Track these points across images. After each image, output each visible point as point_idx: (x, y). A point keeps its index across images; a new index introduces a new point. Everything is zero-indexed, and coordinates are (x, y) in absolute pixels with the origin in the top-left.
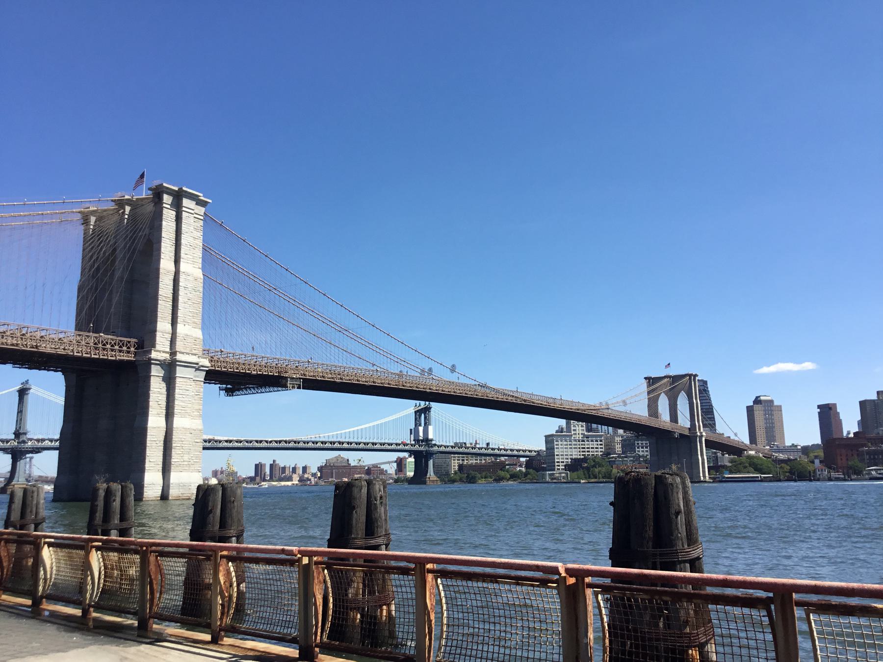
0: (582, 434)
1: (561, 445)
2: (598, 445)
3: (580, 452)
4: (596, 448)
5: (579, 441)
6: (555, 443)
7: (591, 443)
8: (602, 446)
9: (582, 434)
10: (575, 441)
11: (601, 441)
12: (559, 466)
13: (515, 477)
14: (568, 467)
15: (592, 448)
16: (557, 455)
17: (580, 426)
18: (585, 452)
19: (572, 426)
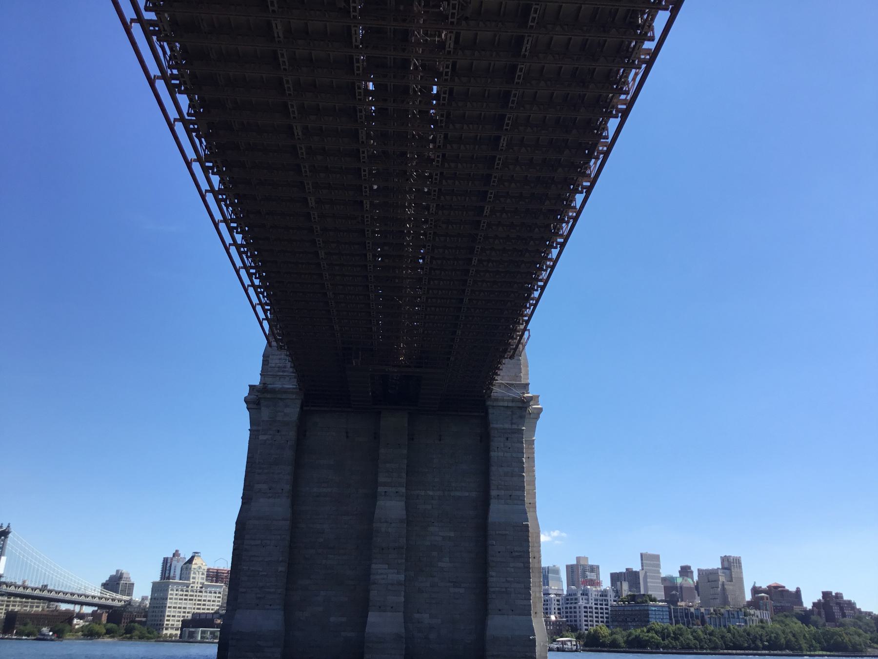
0: (201, 583)
1: (176, 595)
2: (215, 597)
3: (195, 604)
4: (213, 601)
5: (196, 592)
6: (170, 592)
7: (209, 594)
8: (219, 599)
9: (201, 583)
10: (192, 591)
11: (220, 593)
12: (168, 620)
13: (113, 632)
14: (185, 624)
15: (209, 601)
16: (169, 607)
17: (201, 573)
18: (200, 605)
19: (192, 572)
